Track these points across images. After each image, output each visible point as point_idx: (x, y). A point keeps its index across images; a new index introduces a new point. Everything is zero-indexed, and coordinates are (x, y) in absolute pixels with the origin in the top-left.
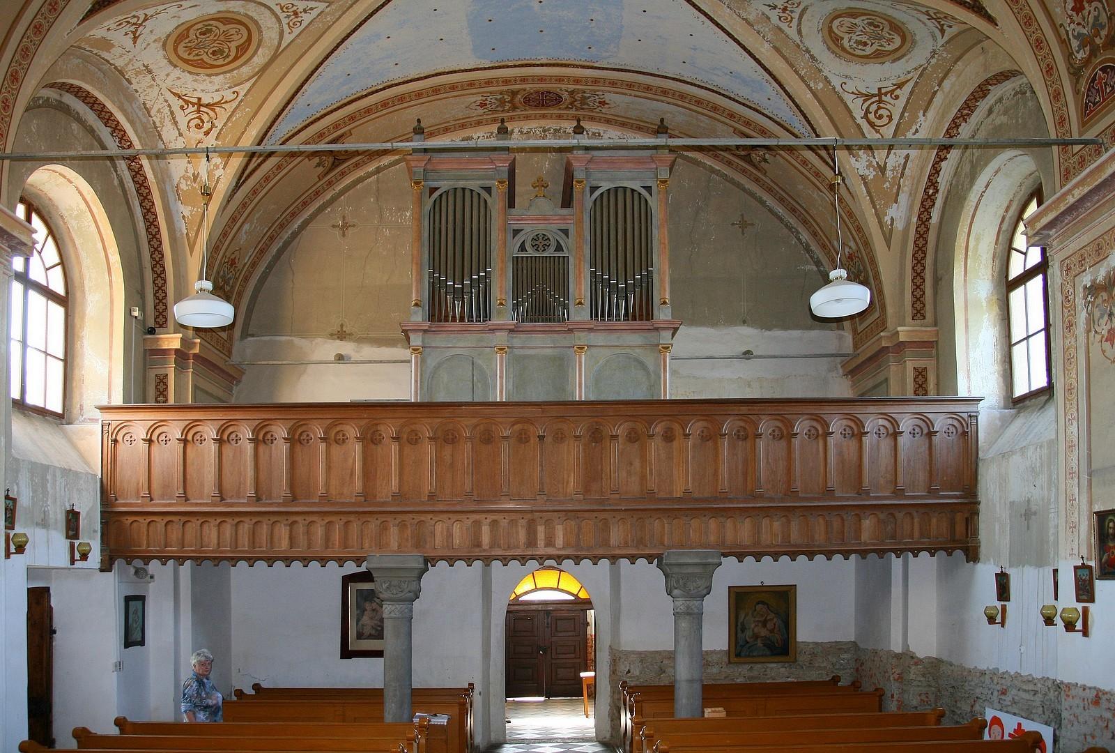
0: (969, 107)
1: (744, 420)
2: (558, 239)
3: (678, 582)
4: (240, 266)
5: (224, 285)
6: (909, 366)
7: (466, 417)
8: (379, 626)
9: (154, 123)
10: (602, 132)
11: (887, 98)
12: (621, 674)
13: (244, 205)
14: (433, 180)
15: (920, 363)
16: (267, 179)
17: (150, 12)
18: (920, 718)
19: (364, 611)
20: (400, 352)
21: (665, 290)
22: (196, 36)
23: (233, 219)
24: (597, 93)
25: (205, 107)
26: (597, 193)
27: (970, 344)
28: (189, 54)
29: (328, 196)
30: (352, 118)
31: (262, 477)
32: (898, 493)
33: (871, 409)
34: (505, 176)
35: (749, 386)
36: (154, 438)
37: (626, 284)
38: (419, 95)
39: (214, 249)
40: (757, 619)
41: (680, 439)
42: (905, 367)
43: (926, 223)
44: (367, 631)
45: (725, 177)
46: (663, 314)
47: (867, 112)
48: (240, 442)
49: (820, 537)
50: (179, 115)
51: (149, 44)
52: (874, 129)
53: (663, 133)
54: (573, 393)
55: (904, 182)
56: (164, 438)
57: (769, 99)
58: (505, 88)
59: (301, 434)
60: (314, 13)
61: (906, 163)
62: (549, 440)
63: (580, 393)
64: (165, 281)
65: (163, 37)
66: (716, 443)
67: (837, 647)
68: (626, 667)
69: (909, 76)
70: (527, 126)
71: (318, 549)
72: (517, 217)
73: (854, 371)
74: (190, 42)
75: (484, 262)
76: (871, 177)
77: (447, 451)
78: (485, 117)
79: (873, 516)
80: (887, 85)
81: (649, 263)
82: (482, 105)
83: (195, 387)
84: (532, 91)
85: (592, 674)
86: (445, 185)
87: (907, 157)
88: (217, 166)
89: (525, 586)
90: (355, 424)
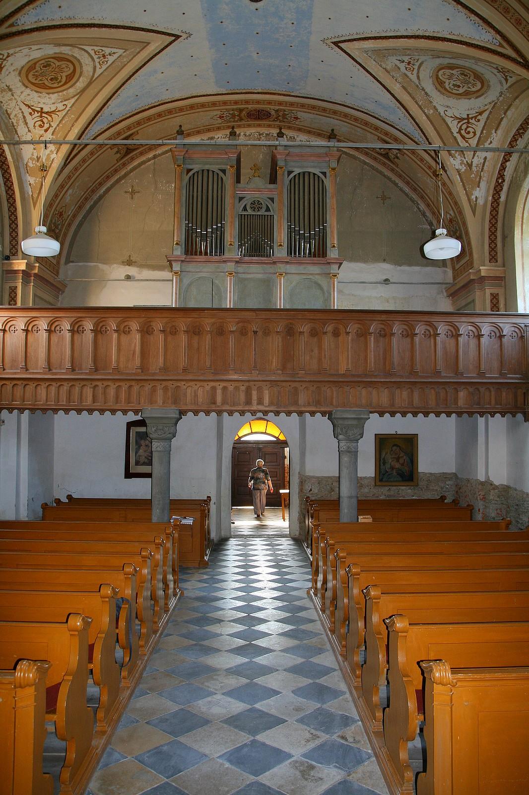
0: (524, 128)
1: (383, 324)
2: (268, 205)
3: (342, 430)
4: (65, 216)
5: (55, 229)
6: (488, 292)
7: (207, 318)
8: (149, 456)
9: (13, 123)
10: (296, 136)
11: (473, 121)
12: (306, 492)
13: (69, 177)
14: (189, 164)
15: (495, 291)
16: (84, 161)
17: (11, 51)
18: (495, 525)
19: (140, 447)
20: (166, 274)
21: (334, 239)
22: (41, 68)
23: (62, 186)
24: (293, 112)
25: (45, 113)
26: (292, 175)
27: (525, 279)
28: (36, 80)
29: (123, 172)
30: (139, 123)
31: (76, 355)
32: (481, 375)
33: (464, 319)
34: (235, 163)
35: (388, 302)
36: (7, 329)
37: (310, 233)
38: (181, 109)
39: (49, 206)
40: (393, 456)
41: (343, 335)
42: (485, 293)
43: (498, 201)
44: (142, 459)
45: (372, 167)
46: (333, 254)
47: (460, 129)
48: (62, 332)
49: (432, 403)
50: (28, 118)
51: (10, 73)
52: (464, 140)
53: (333, 138)
54: (276, 304)
55: (483, 174)
56: (13, 329)
57: (400, 119)
58: (235, 107)
59: (101, 327)
60: (116, 56)
61: (484, 162)
62: (260, 333)
63: (280, 304)
64: (17, 226)
65: (19, 68)
66: (366, 338)
67: (444, 477)
68: (309, 487)
69: (486, 107)
70: (249, 131)
71: (111, 404)
72: (242, 189)
73: (453, 294)
74: (36, 72)
75: (221, 218)
76: (463, 170)
77: (196, 339)
78: (223, 125)
79: (465, 389)
80: (473, 113)
81: (324, 221)
82: (221, 117)
83: (35, 295)
84: (252, 109)
85: (287, 491)
86: (196, 168)
87: (485, 158)
88: (51, 151)
89: (244, 431)
90: (136, 321)
